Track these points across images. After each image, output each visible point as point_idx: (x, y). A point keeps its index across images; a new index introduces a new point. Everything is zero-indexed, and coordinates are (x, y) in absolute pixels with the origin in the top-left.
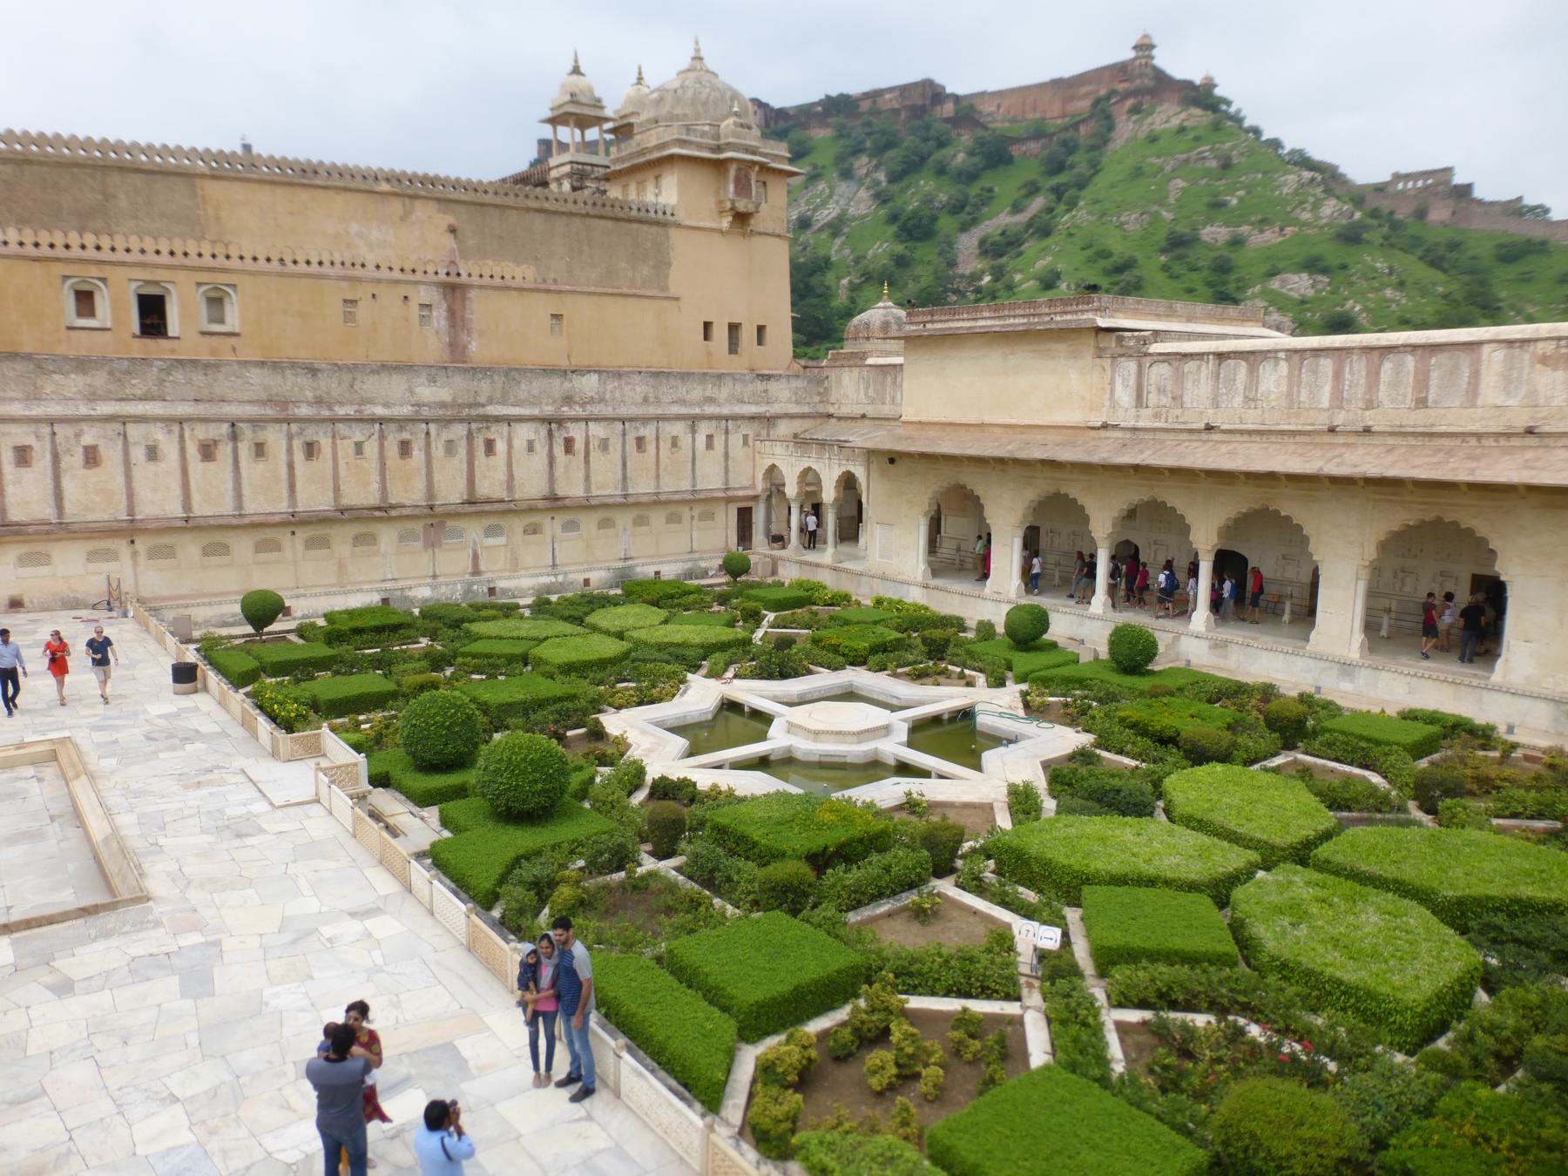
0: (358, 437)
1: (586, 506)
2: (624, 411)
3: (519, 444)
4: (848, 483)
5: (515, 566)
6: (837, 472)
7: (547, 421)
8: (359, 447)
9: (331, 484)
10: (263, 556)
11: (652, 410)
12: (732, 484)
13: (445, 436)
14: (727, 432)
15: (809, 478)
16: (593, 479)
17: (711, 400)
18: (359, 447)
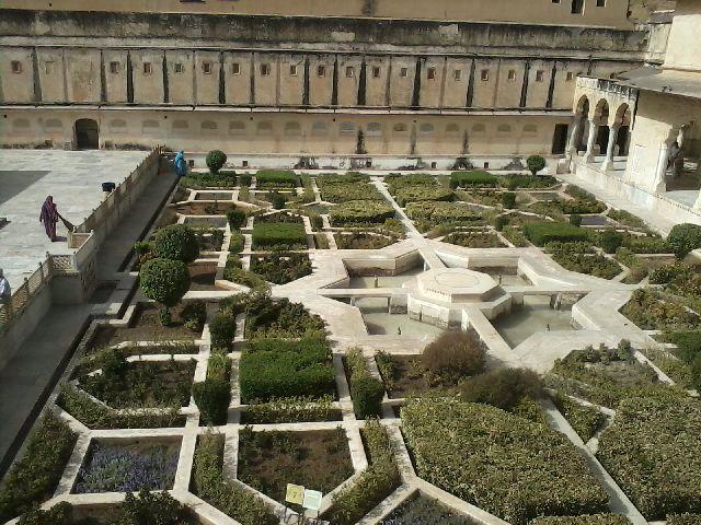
0: (294, 63)
1: (439, 113)
2: (473, 51)
3: (396, 71)
4: (623, 109)
5: (385, 153)
6: (619, 103)
7: (419, 57)
8: (293, 69)
9: (274, 88)
10: (234, 131)
11: (495, 52)
12: (258, 101)
13: (348, 64)
14: (554, 71)
15: (603, 108)
16: (446, 97)
17: (543, 48)
18: (293, 69)
